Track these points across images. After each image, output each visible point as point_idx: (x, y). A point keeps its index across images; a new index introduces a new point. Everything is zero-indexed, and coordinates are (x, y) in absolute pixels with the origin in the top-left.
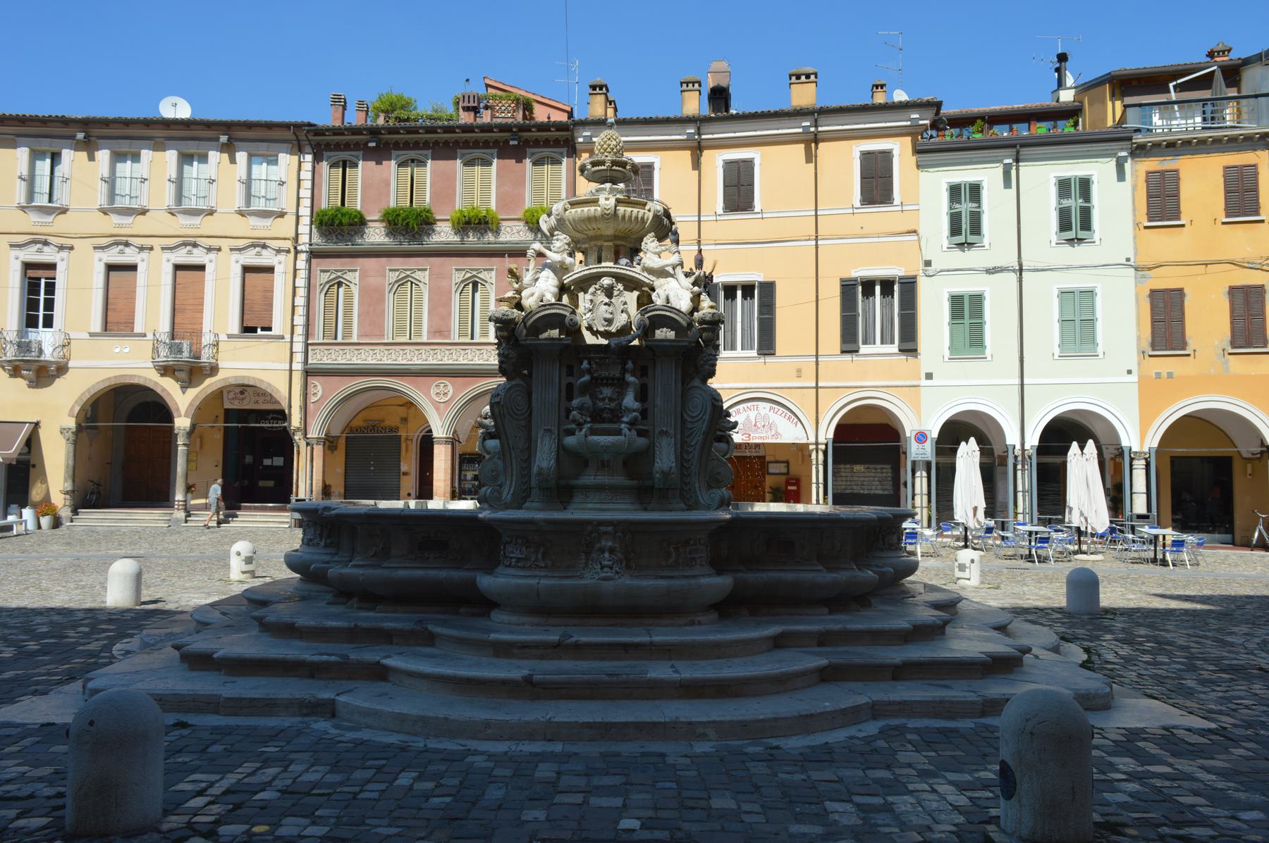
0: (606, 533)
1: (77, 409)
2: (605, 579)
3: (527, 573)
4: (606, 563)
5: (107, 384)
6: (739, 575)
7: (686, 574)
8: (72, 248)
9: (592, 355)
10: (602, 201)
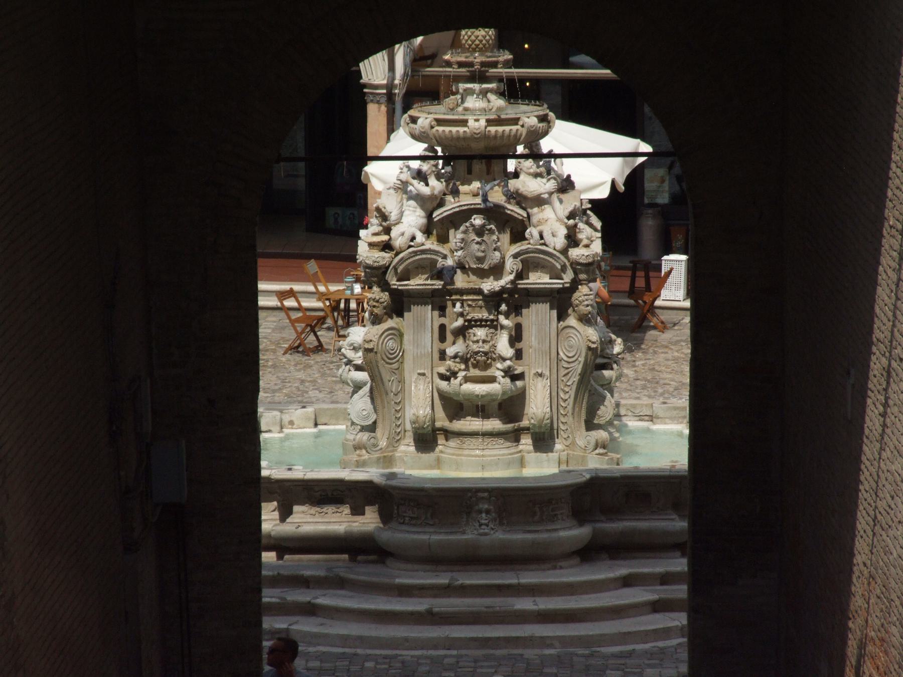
0: (483, 498)
2: (481, 535)
3: (420, 530)
4: (483, 522)
6: (599, 525)
7: (549, 528)
9: (465, 298)
10: (471, 123)
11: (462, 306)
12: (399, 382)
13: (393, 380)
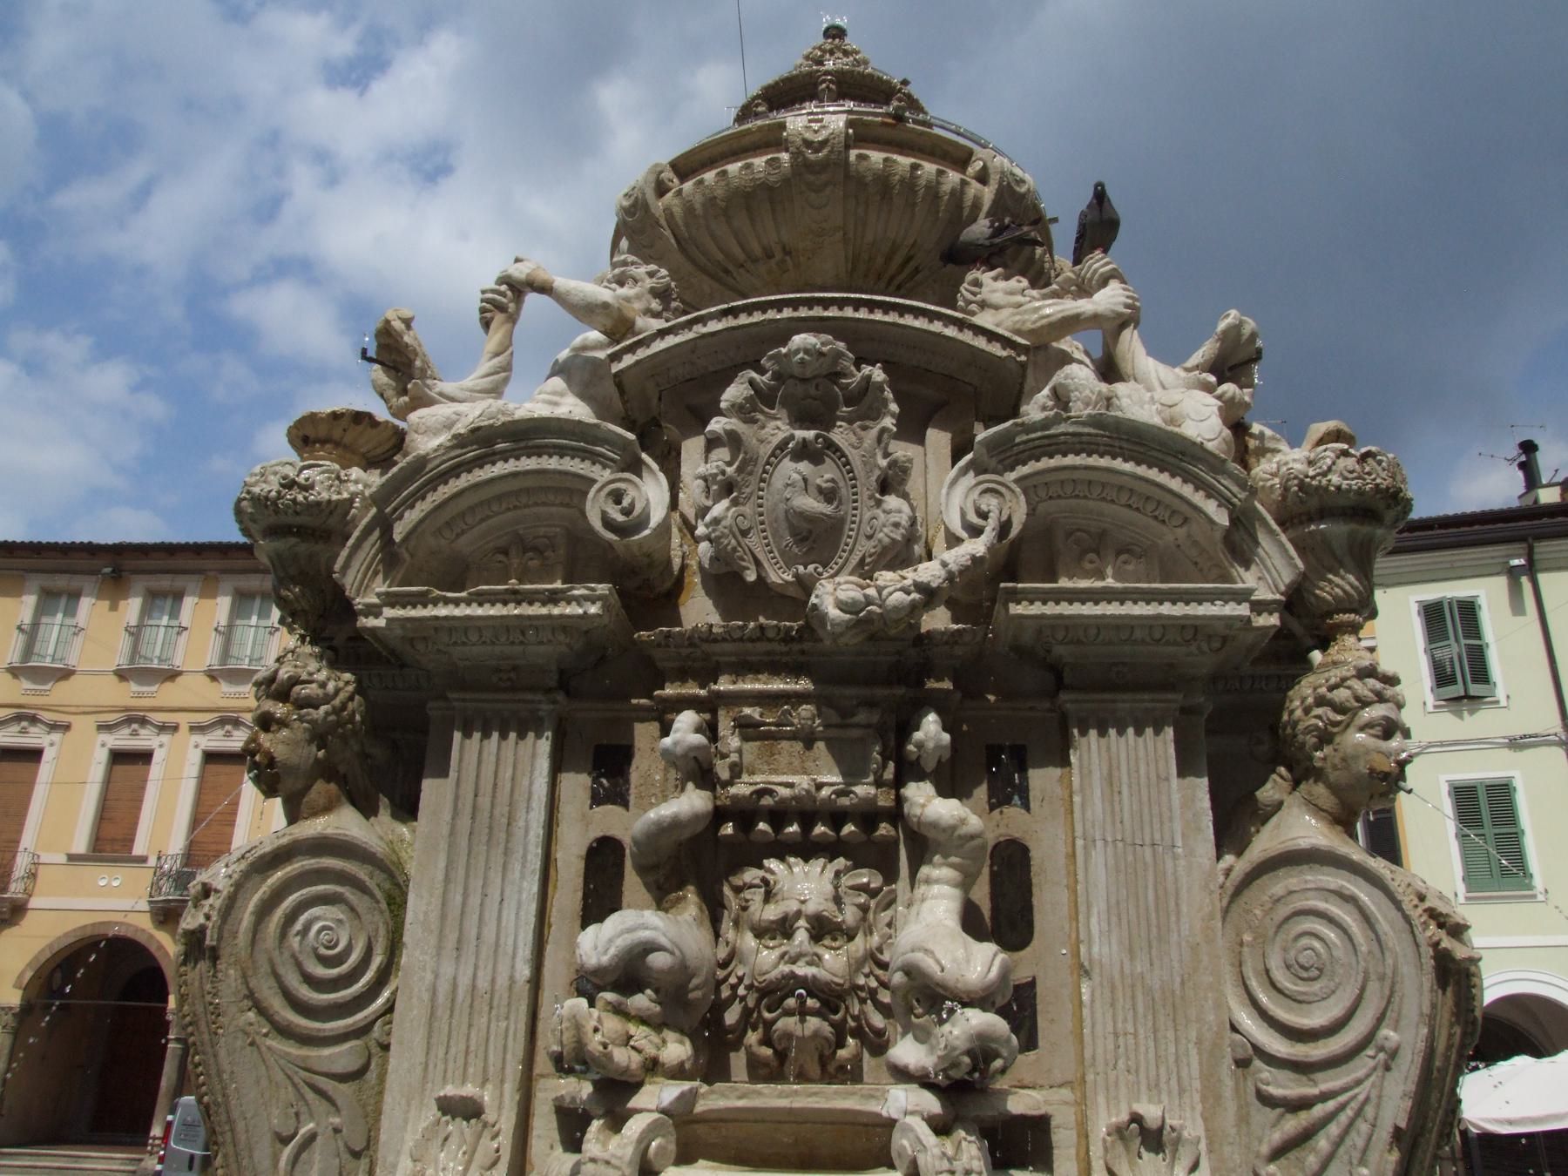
1: (29, 974)
5: (80, 935)
8: (67, 728)
9: (724, 685)
11: (710, 730)
12: (356, 1155)
13: (312, 1137)
